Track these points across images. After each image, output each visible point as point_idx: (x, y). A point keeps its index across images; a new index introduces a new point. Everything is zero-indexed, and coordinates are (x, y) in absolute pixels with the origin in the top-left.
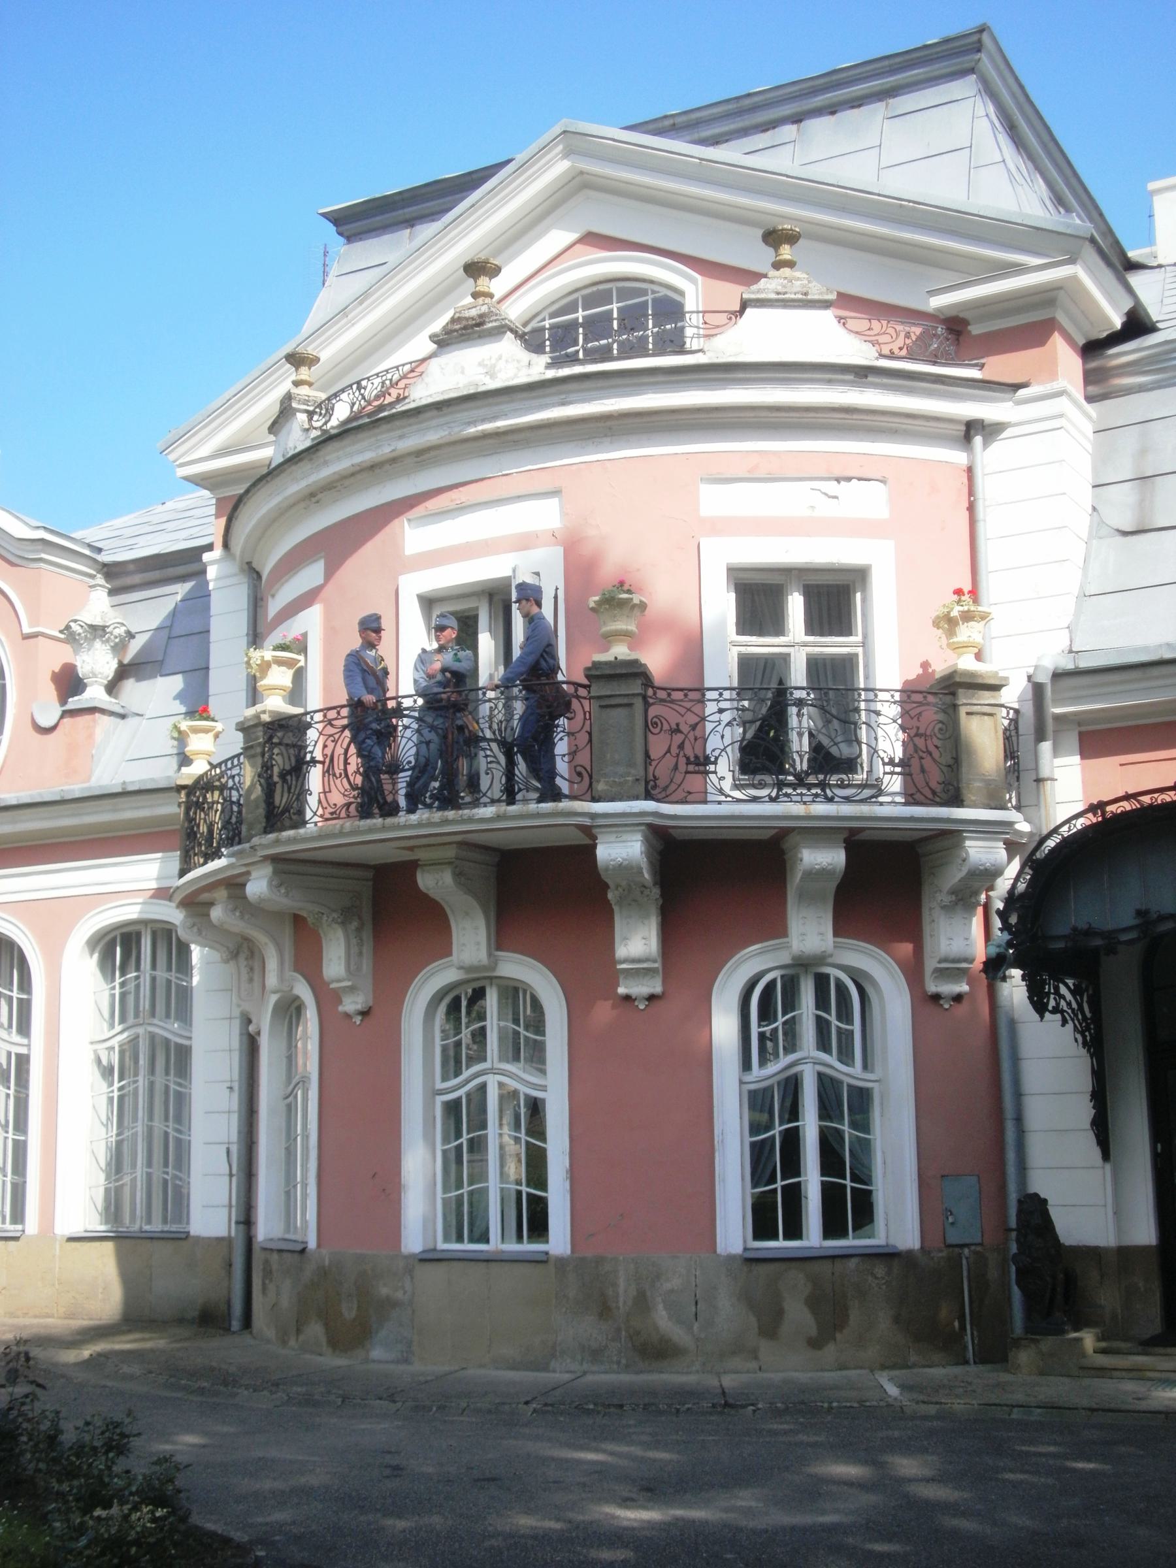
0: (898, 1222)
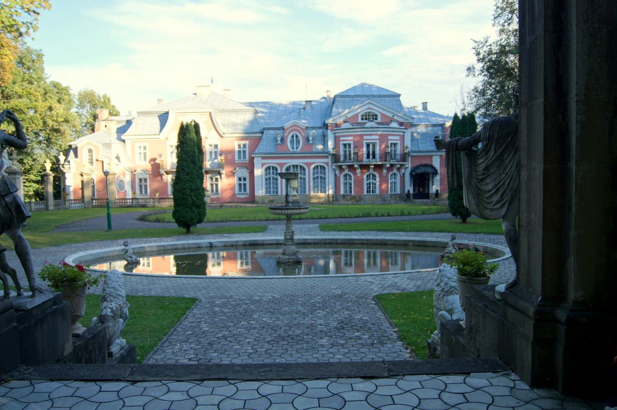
0: (398, 192)
